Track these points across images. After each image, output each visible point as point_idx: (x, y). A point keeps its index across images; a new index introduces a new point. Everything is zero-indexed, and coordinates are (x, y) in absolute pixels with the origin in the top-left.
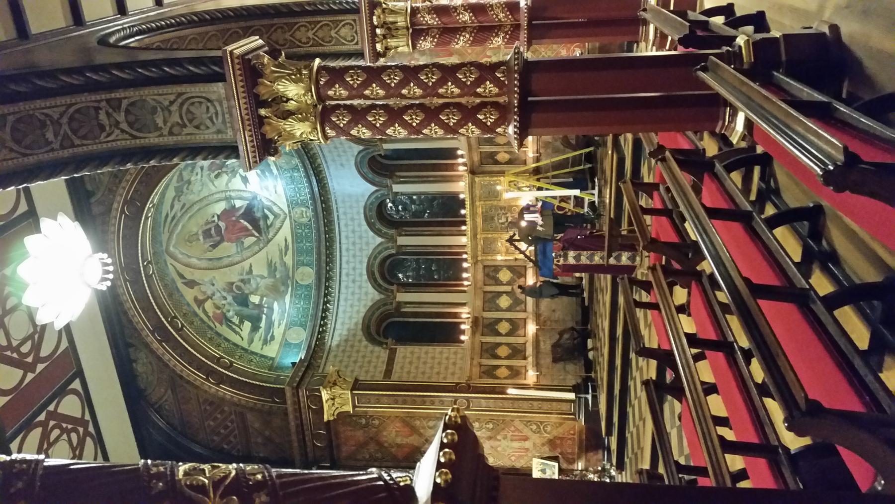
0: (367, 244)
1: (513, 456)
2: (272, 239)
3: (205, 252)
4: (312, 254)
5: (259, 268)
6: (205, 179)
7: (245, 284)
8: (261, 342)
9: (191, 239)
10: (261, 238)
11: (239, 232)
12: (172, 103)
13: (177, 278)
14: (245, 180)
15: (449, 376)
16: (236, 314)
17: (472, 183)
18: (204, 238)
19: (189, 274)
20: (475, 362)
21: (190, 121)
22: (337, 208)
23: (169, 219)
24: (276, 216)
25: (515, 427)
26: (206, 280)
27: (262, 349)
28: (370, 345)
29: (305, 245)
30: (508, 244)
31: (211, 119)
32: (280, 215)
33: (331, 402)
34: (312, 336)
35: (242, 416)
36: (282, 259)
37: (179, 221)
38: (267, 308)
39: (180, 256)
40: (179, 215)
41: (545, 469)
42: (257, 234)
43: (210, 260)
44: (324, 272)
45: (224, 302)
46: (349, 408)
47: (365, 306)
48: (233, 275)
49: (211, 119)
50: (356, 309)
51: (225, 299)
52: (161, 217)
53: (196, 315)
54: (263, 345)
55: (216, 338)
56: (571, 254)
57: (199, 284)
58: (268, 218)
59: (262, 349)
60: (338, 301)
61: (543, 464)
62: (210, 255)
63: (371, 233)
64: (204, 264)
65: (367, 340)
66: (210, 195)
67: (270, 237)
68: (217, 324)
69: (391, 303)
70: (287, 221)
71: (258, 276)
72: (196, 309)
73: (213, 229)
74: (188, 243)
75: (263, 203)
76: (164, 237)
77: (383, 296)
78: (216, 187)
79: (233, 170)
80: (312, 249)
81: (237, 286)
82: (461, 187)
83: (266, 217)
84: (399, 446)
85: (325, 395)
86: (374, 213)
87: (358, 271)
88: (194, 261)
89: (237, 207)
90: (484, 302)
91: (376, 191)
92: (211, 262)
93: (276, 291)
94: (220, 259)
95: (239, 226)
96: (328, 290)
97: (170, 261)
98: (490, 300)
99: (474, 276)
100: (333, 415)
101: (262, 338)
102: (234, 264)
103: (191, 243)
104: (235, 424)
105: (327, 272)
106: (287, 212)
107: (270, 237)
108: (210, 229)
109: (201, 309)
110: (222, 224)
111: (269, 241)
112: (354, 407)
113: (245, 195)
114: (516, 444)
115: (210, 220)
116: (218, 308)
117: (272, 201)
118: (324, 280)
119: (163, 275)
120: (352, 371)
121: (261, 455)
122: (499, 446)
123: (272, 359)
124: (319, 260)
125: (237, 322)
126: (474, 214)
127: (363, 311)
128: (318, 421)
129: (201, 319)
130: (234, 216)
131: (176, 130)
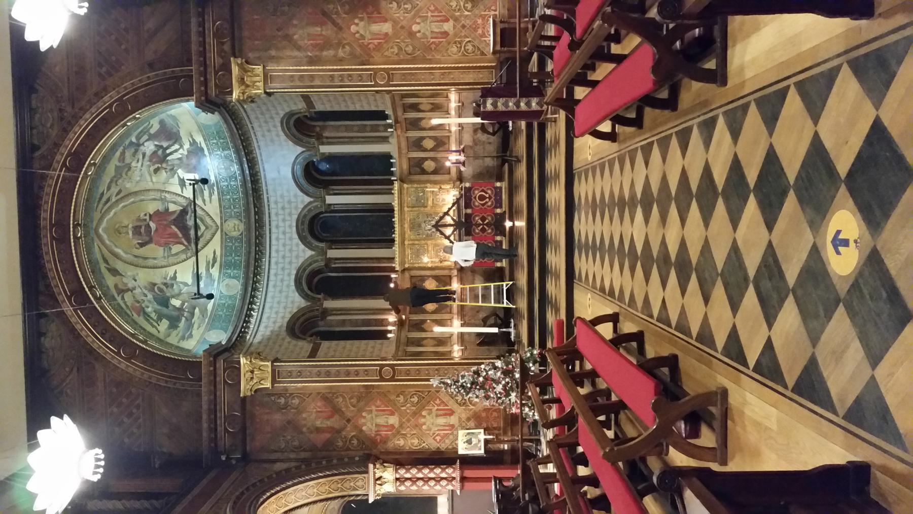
0: (297, 257)
1: (437, 435)
4: (240, 267)
6: (144, 168)
7: (167, 287)
10: (190, 248)
11: (168, 238)
13: (101, 261)
16: (155, 311)
17: (401, 190)
22: (270, 221)
23: (104, 199)
25: (440, 399)
27: (178, 342)
29: (233, 258)
30: (434, 230)
32: (212, 226)
36: (208, 270)
38: (188, 312)
39: (107, 242)
40: (114, 199)
41: (471, 439)
42: (186, 243)
43: (136, 256)
46: (268, 384)
47: (290, 312)
48: (157, 276)
50: (280, 315)
53: (115, 300)
56: (490, 101)
57: (121, 275)
58: (200, 229)
59: (178, 342)
60: (263, 309)
61: (468, 434)
63: (302, 246)
68: (133, 313)
70: (218, 236)
71: (181, 283)
72: (116, 295)
73: (143, 227)
74: (116, 232)
76: (96, 216)
77: (309, 304)
79: (172, 169)
80: (241, 262)
81: (159, 288)
83: (196, 227)
84: (318, 430)
85: (243, 361)
86: (306, 226)
87: (285, 283)
88: (119, 251)
89: (170, 210)
91: (310, 203)
94: (146, 258)
95: (169, 231)
96: (253, 299)
97: (97, 243)
100: (251, 390)
102: (159, 268)
103: (120, 234)
109: (120, 296)
110: (153, 225)
112: (274, 381)
113: (180, 200)
114: (441, 421)
116: (138, 302)
117: (205, 211)
118: (250, 289)
122: (424, 424)
123: (189, 351)
125: (155, 318)
127: (288, 316)
129: (119, 304)
130: (165, 220)
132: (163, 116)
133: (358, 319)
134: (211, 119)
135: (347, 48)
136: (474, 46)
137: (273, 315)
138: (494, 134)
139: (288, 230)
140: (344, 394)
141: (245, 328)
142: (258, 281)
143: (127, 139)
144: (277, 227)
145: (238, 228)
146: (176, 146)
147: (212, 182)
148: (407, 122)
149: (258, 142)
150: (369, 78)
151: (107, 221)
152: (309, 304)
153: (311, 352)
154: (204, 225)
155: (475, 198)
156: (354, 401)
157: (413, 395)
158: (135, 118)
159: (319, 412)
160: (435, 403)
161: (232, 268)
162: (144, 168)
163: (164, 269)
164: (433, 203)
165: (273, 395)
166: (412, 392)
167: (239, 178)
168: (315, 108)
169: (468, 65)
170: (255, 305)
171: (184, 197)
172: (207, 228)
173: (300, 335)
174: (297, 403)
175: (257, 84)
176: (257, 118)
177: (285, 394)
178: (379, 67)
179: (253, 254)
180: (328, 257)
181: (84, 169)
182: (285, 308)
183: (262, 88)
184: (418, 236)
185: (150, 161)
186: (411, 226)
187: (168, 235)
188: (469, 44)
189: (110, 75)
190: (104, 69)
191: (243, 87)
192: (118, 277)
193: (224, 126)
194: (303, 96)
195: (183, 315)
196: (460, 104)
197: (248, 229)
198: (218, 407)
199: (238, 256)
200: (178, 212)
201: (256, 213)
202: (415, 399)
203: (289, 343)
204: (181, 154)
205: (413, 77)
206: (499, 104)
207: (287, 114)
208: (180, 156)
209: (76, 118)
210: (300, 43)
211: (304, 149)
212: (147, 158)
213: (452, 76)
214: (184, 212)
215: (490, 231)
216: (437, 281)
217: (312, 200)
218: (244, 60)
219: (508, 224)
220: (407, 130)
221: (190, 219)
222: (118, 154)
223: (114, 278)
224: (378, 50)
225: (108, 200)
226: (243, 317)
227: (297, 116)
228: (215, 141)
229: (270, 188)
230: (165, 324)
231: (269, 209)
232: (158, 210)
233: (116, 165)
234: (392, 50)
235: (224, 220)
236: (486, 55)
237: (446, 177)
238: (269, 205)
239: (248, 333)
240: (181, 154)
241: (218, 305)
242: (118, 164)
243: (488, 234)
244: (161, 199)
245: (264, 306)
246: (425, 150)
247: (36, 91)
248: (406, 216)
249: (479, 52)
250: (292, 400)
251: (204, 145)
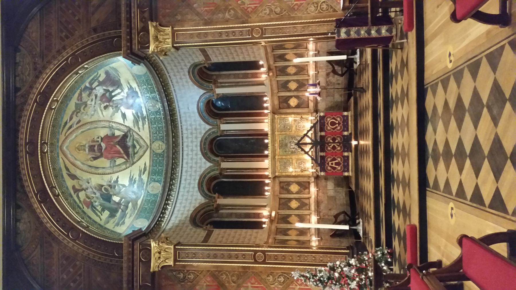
0: (200, 167)
2: (136, 162)
3: (88, 160)
4: (162, 174)
6: (97, 106)
7: (111, 188)
8: (114, 224)
9: (81, 148)
10: (129, 161)
11: (114, 154)
14: (124, 116)
16: (100, 205)
17: (273, 119)
18: (89, 151)
20: (272, 236)
22: (183, 143)
26: (84, 178)
28: (194, 228)
30: (296, 147)
32: (144, 146)
33: (157, 255)
34: (152, 222)
36: (140, 176)
38: (124, 205)
39: (69, 156)
40: (75, 127)
42: (126, 157)
43: (90, 166)
44: (168, 185)
45: (93, 195)
46: (171, 263)
47: (194, 207)
48: (104, 180)
50: (187, 209)
51: (95, 194)
52: (62, 121)
53: (72, 197)
54: (115, 226)
55: (81, 213)
56: (343, 30)
57: (78, 179)
58: (136, 147)
60: (176, 204)
63: (204, 160)
64: (85, 168)
65: (192, 226)
66: (99, 121)
67: (135, 160)
68: (84, 206)
69: (213, 205)
70: (148, 152)
71: (121, 185)
73: (96, 146)
74: (77, 150)
75: (133, 135)
76: (62, 137)
77: (207, 201)
78: (104, 116)
79: (116, 107)
80: (162, 171)
81: (105, 188)
82: (265, 126)
83: (134, 147)
85: (153, 244)
87: (192, 186)
88: (78, 163)
89: (116, 135)
90: (279, 204)
91: (210, 129)
92: (90, 168)
94: (97, 168)
95: (114, 149)
97: (61, 155)
98: (284, 204)
99: (273, 188)
100: (158, 267)
101: (116, 222)
102: (107, 174)
104: (82, 278)
106: (149, 144)
107: (135, 160)
108: (94, 146)
109: (76, 194)
110: (103, 145)
111: (133, 163)
112: (175, 261)
116: (89, 198)
117: (140, 136)
118: (167, 190)
119: (54, 161)
124: (166, 178)
125: (100, 210)
126: (273, 141)
128: (146, 273)
132: (107, 68)
133: (242, 213)
134: (140, 69)
135: (232, 12)
136: (326, 5)
137: (182, 209)
138: (342, 75)
139: (194, 148)
140: (227, 273)
141: (161, 218)
142: (173, 184)
143: (83, 84)
145: (161, 147)
146: (119, 91)
147: (144, 115)
148: (277, 69)
149: (174, 87)
150: (248, 33)
151: (70, 141)
152: (207, 201)
153: (205, 238)
154: (139, 145)
155: (328, 124)
156: (235, 278)
157: (280, 275)
158: (83, 67)
159: (208, 285)
160: (297, 283)
161: (157, 175)
162: (97, 106)
163: (110, 175)
164: (296, 128)
165: (175, 271)
166: (279, 273)
167: (162, 113)
168: (211, 61)
169: (323, 20)
170: (170, 201)
171: (126, 126)
172: (141, 147)
173: (199, 225)
174: (192, 278)
175: (167, 40)
176: (172, 69)
177: (184, 270)
178: (255, 24)
179: (171, 165)
180: (221, 167)
181: (49, 104)
182: (190, 203)
183: (171, 43)
184: (285, 153)
185: (101, 100)
186: (280, 145)
187: (114, 151)
188: (323, 4)
189: (67, 37)
190: (64, 34)
191: (157, 43)
193: (150, 76)
194: (200, 49)
195: (120, 208)
196: (316, 52)
197: (168, 148)
198: (135, 279)
199: (161, 166)
200: (121, 136)
201: (173, 137)
202: (282, 279)
203: (191, 229)
204: (122, 96)
205: (280, 31)
206: (352, 33)
207: (192, 65)
208: (122, 97)
209: (44, 68)
210: (199, 10)
211: (206, 91)
212: (98, 98)
213: (310, 29)
214: (125, 136)
215: (339, 148)
216: (299, 185)
217: (211, 127)
218: (158, 23)
219: (354, 143)
220: (277, 76)
221: (129, 141)
222: (76, 95)
224: (255, 12)
225: (71, 127)
226: (161, 210)
227: (199, 67)
228: (145, 87)
229: (183, 119)
230: (107, 213)
231: (182, 134)
232: (107, 135)
233: (75, 102)
234: (265, 12)
235: (152, 142)
236: (337, 12)
237: (306, 110)
238: (182, 131)
239: (163, 221)
240: (122, 96)
241: (145, 201)
242: (77, 102)
243: (338, 150)
244: (110, 127)
245: (176, 201)
246: (290, 91)
247: (19, 51)
248: (277, 138)
249: (332, 10)
250: (188, 275)
251: (137, 90)
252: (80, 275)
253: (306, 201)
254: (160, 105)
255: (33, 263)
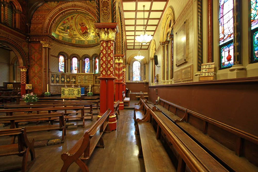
3: (79, 22)
5: (75, 33)
6: (93, 25)
9: (81, 20)
12: (108, 11)
13: (73, 15)
14: (93, 33)
15: (52, 68)
16: (65, 26)
19: (74, 18)
20: (55, 73)
21: (104, 14)
24: (86, 37)
31: (105, 19)
35: (41, 23)
36: (77, 37)
37: (85, 18)
49: (105, 19)
53: (65, 18)
57: (72, 20)
61: (31, 86)
62: (78, 23)
63: (82, 55)
70: (85, 40)
76: (82, 15)
83: (86, 35)
84: (35, 57)
88: (77, 20)
93: (70, 35)
94: (77, 25)
97: (77, 15)
105: (74, 46)
110: (84, 27)
111: (81, 35)
112: (44, 48)
113: (90, 32)
114: (36, 81)
115: (85, 25)
116: (67, 23)
120: (52, 48)
121: (31, 26)
124: (77, 45)
131: (103, 11)
139: (86, 53)
144: (86, 51)
156: (40, 64)
167: (95, 43)
192: (71, 19)
203: (58, 52)
223: (71, 18)
237: (94, 83)
252: (40, 21)
253: (69, 83)
254: (97, 43)
255: (43, 7)
